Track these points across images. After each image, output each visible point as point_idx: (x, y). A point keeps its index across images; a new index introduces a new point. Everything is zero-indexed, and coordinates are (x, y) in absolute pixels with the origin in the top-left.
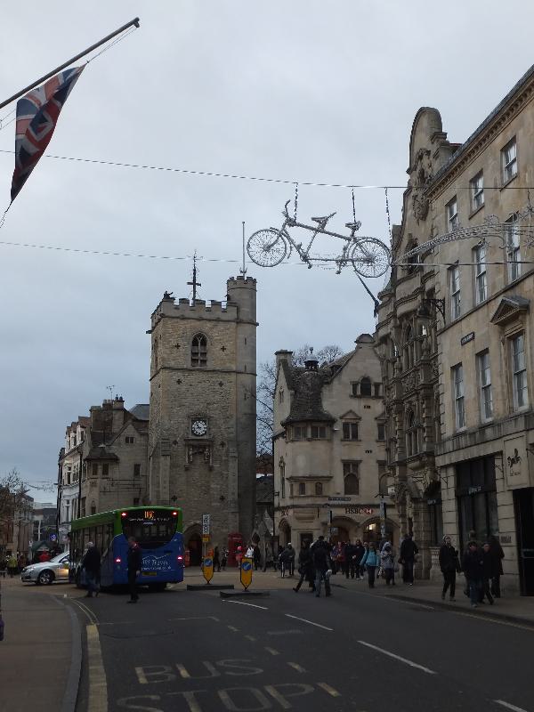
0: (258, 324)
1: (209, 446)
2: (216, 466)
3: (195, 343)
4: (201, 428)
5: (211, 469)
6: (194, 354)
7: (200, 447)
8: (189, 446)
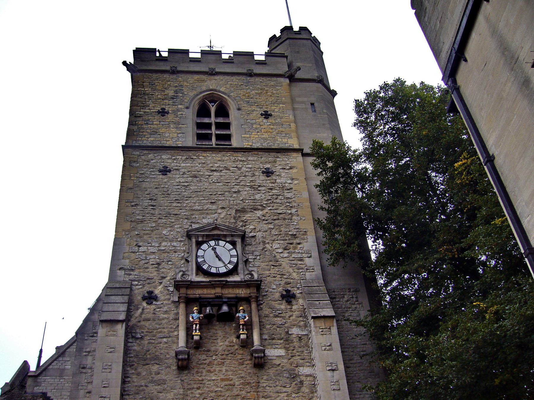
0: (334, 93)
1: (247, 300)
2: (274, 353)
3: (203, 111)
4: (219, 257)
5: (260, 363)
6: (200, 126)
7: (217, 302)
8: (189, 302)
